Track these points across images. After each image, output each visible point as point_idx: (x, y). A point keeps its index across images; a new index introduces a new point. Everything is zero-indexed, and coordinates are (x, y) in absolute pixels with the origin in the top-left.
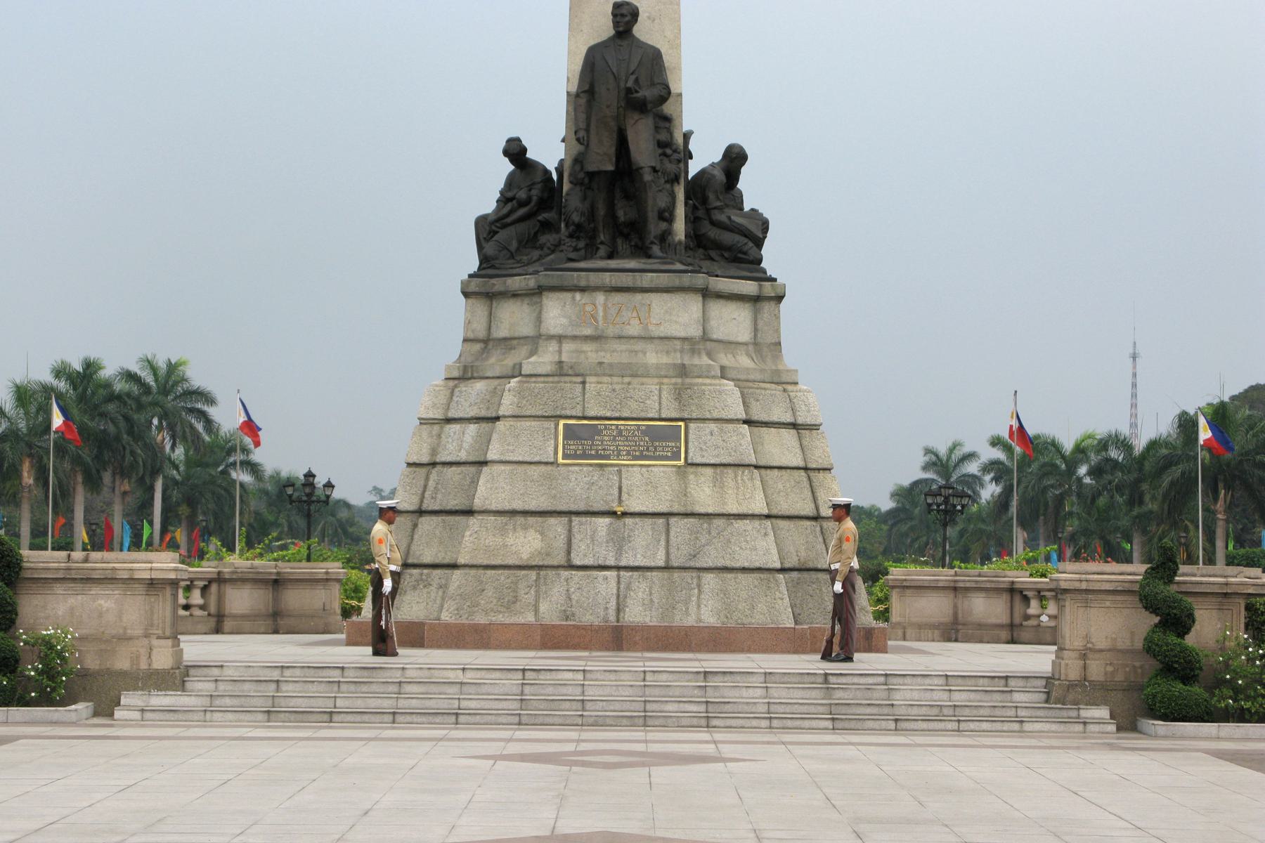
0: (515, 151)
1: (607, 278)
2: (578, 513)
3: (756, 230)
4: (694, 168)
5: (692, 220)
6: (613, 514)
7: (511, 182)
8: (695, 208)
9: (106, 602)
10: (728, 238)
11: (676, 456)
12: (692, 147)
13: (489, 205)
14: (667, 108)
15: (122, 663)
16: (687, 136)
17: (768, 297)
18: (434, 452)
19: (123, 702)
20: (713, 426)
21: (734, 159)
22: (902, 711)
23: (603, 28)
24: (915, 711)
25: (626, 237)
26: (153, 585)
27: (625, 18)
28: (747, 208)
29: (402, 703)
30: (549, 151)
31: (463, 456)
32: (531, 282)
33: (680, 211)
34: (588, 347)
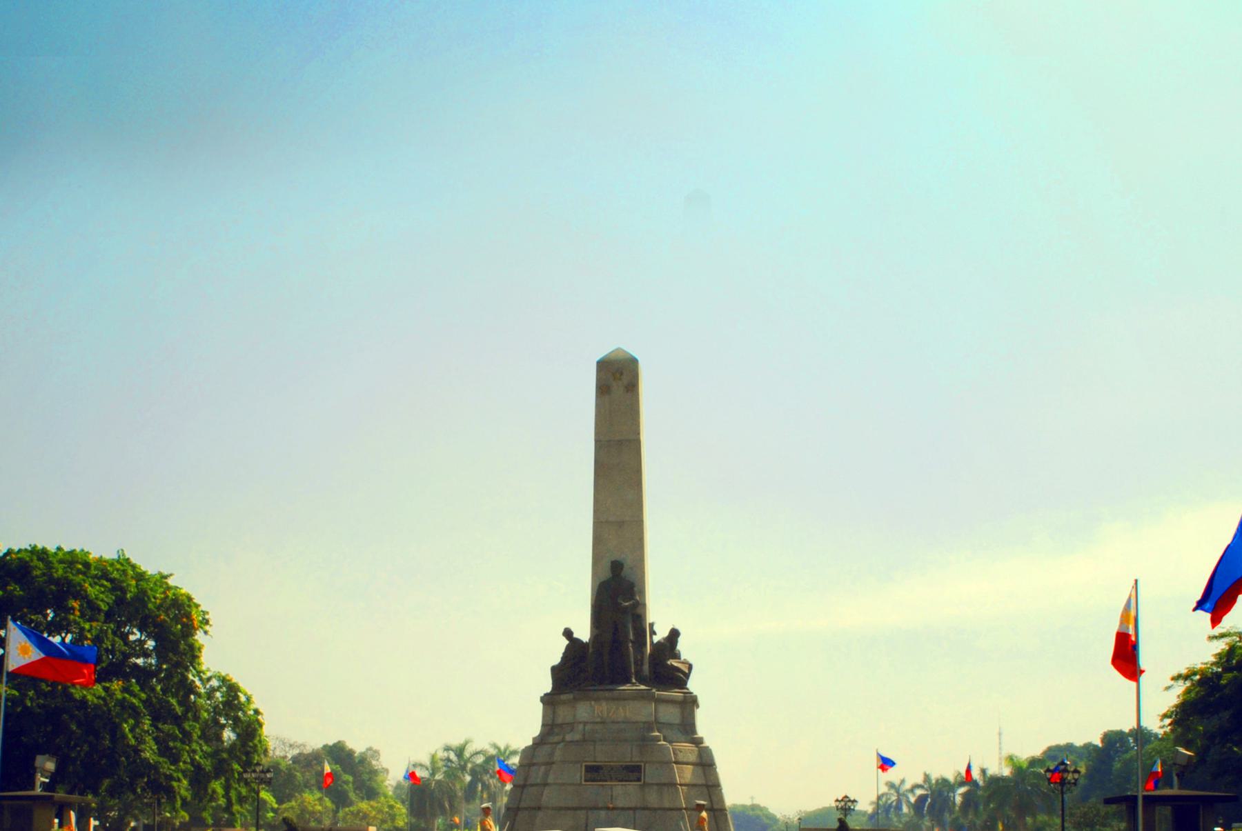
0: (568, 633)
1: (607, 694)
2: (591, 809)
4: (656, 639)
6: (608, 808)
7: (568, 648)
11: (639, 780)
12: (655, 628)
13: (556, 659)
14: (639, 611)
16: (652, 625)
17: (691, 702)
18: (526, 780)
21: (674, 634)
23: (606, 574)
27: (617, 567)
28: (683, 658)
30: (584, 633)
31: (538, 781)
32: (571, 696)
34: (598, 727)
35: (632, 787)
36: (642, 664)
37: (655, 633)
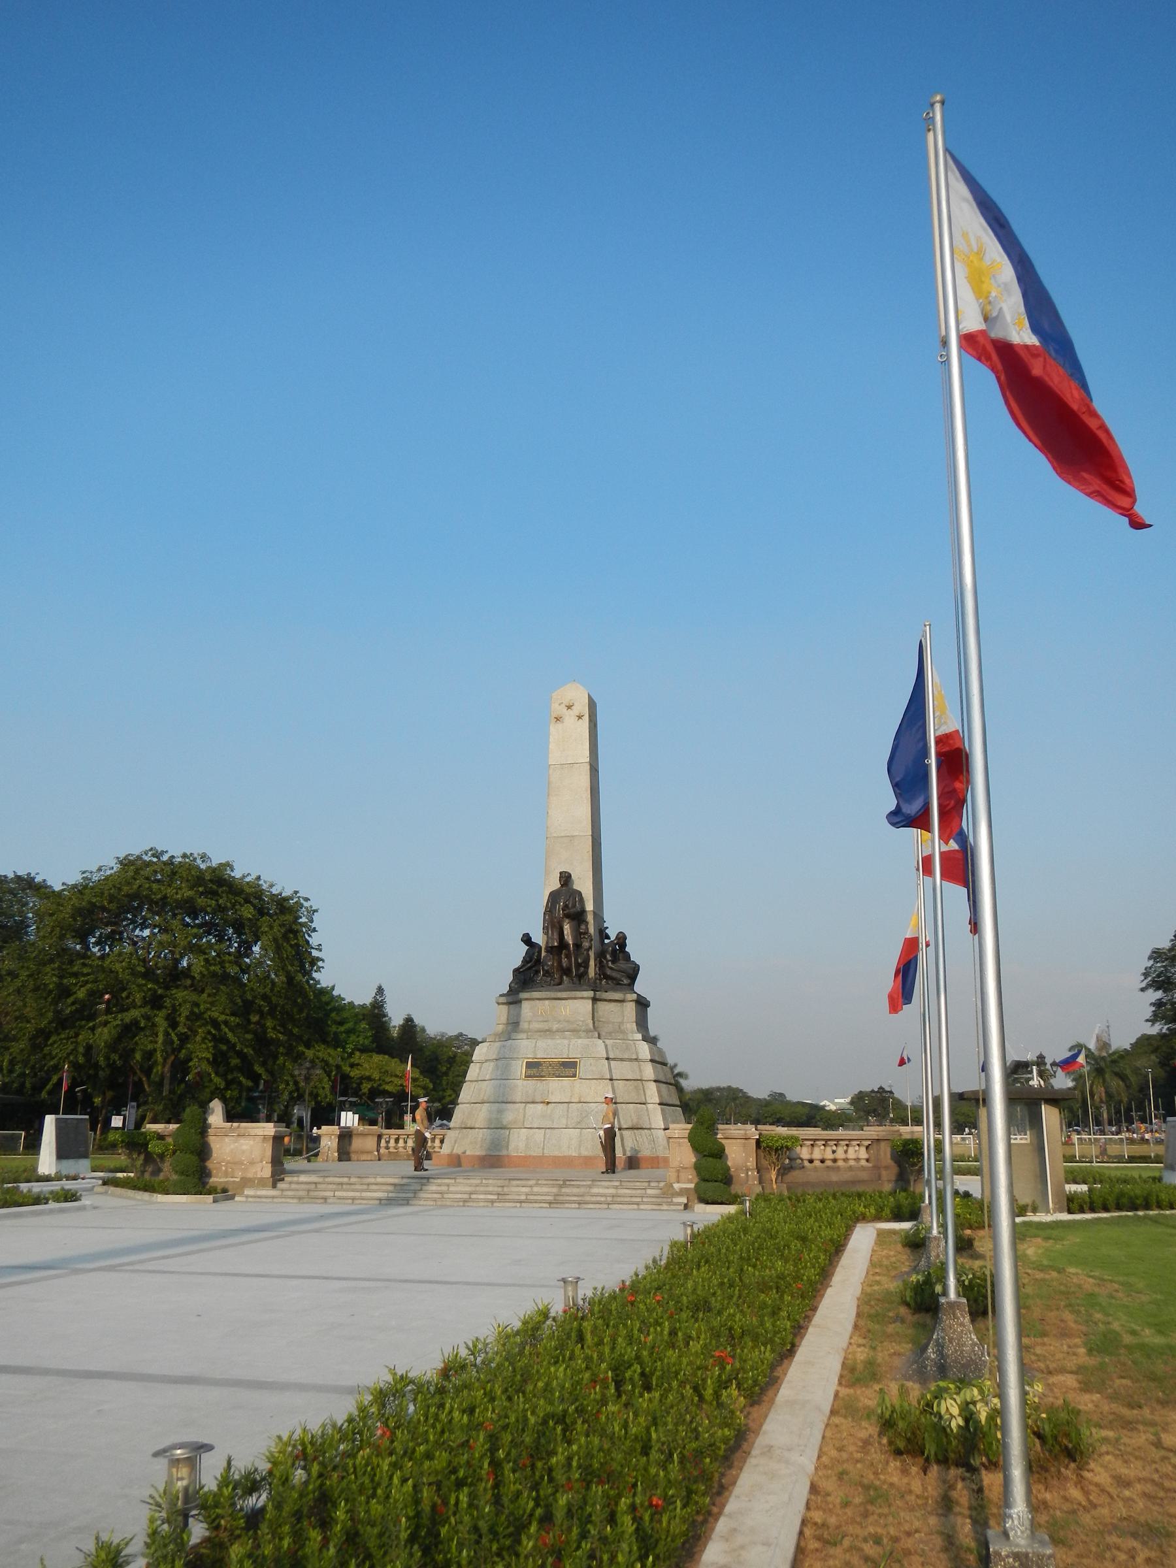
0: (527, 939)
3: (633, 973)
5: (601, 966)
8: (601, 962)
9: (246, 1145)
10: (614, 974)
13: (518, 963)
15: (250, 1175)
19: (246, 1193)
20: (591, 1060)
21: (622, 939)
22: (588, 1198)
24: (594, 1199)
25: (567, 976)
26: (265, 1138)
29: (364, 1194)
31: (488, 1077)
33: (592, 963)
35: (566, 1081)
36: (587, 967)
37: (608, 938)
